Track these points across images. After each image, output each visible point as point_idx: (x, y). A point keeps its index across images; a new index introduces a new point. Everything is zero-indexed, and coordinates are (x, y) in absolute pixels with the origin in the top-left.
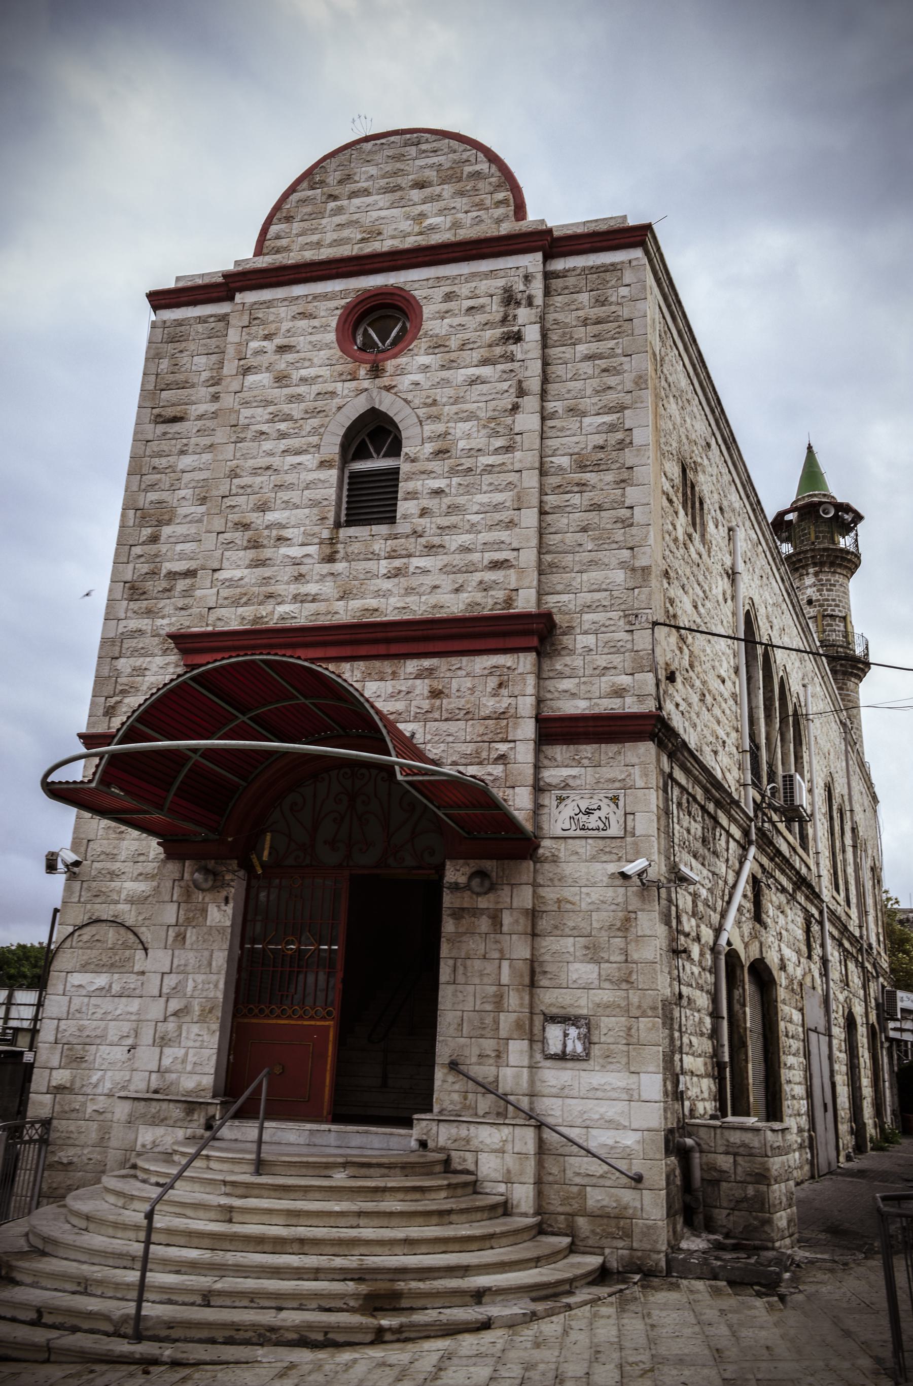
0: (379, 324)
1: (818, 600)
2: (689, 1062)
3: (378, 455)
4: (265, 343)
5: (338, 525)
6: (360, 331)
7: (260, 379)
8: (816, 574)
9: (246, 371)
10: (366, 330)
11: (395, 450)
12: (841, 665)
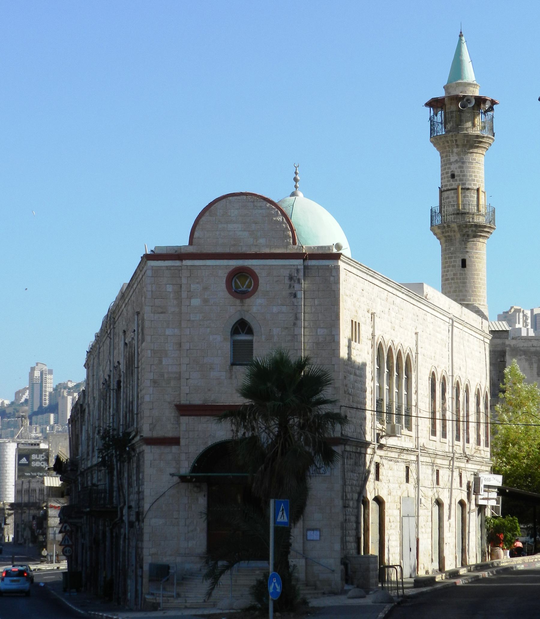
0: (242, 283)
1: (459, 176)
2: (348, 538)
3: (243, 333)
4: (198, 285)
5: (233, 364)
6: (233, 281)
7: (196, 302)
8: (458, 154)
9: (190, 298)
10: (236, 282)
11: (250, 331)
12: (472, 231)
